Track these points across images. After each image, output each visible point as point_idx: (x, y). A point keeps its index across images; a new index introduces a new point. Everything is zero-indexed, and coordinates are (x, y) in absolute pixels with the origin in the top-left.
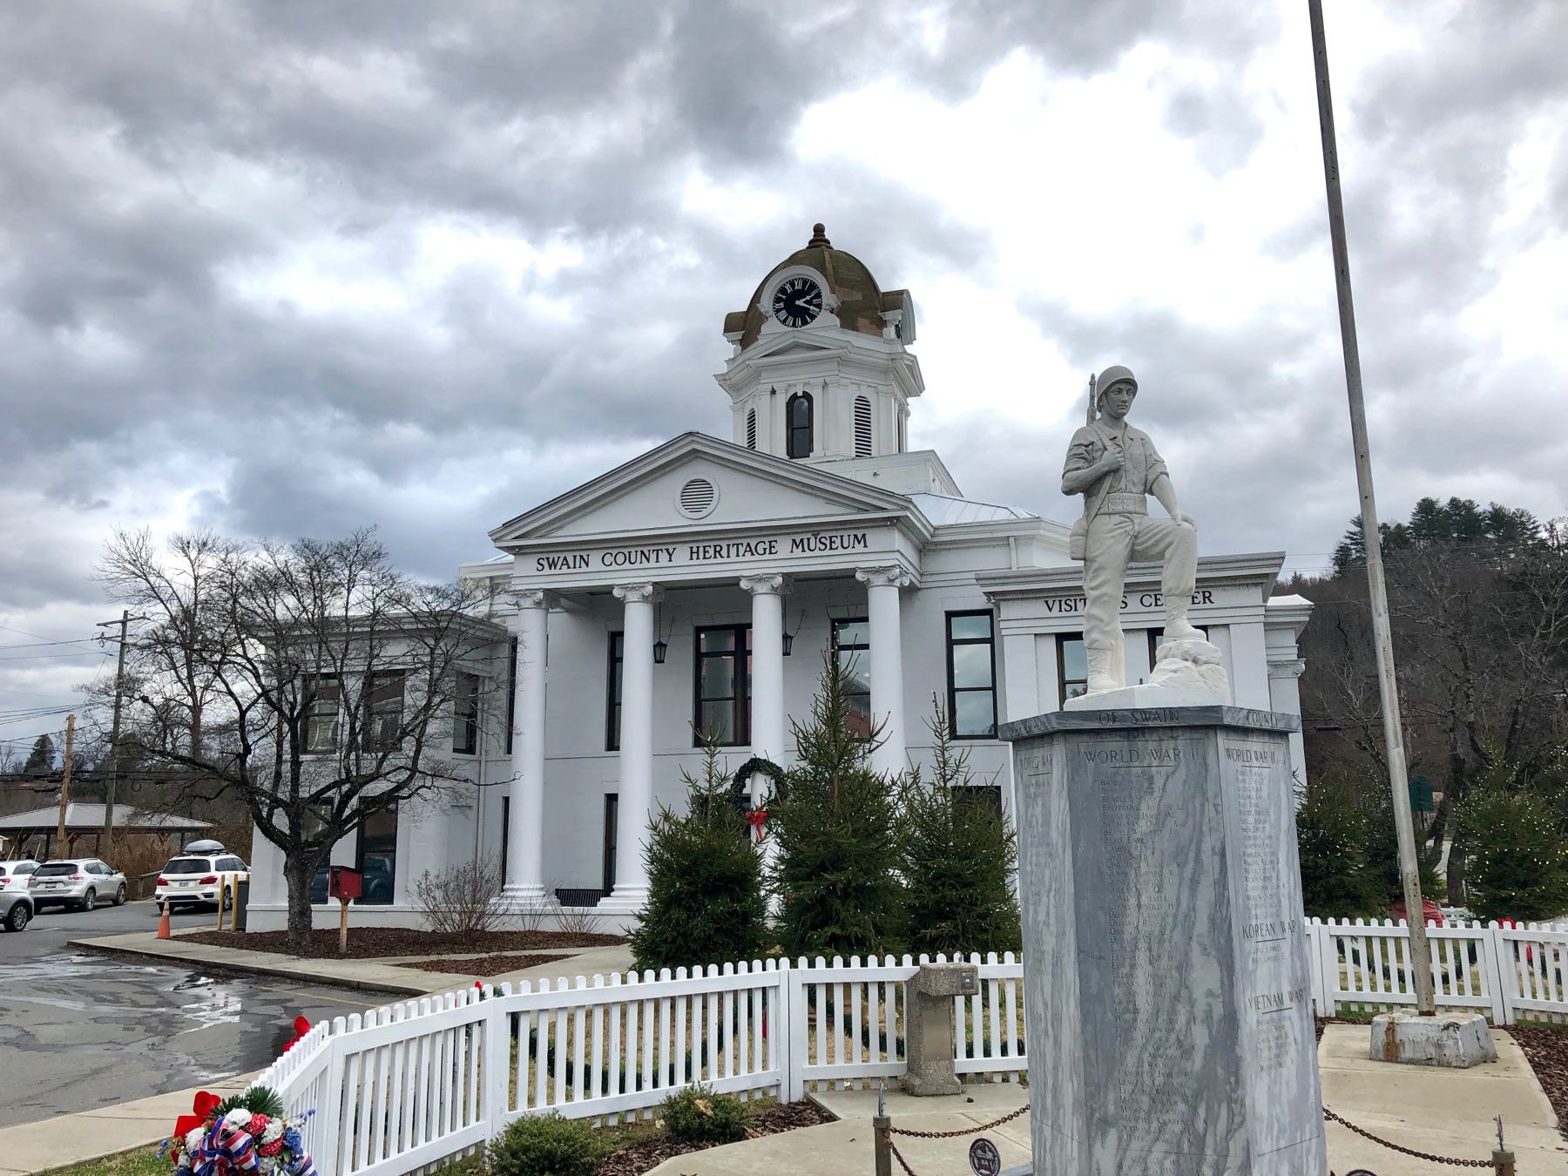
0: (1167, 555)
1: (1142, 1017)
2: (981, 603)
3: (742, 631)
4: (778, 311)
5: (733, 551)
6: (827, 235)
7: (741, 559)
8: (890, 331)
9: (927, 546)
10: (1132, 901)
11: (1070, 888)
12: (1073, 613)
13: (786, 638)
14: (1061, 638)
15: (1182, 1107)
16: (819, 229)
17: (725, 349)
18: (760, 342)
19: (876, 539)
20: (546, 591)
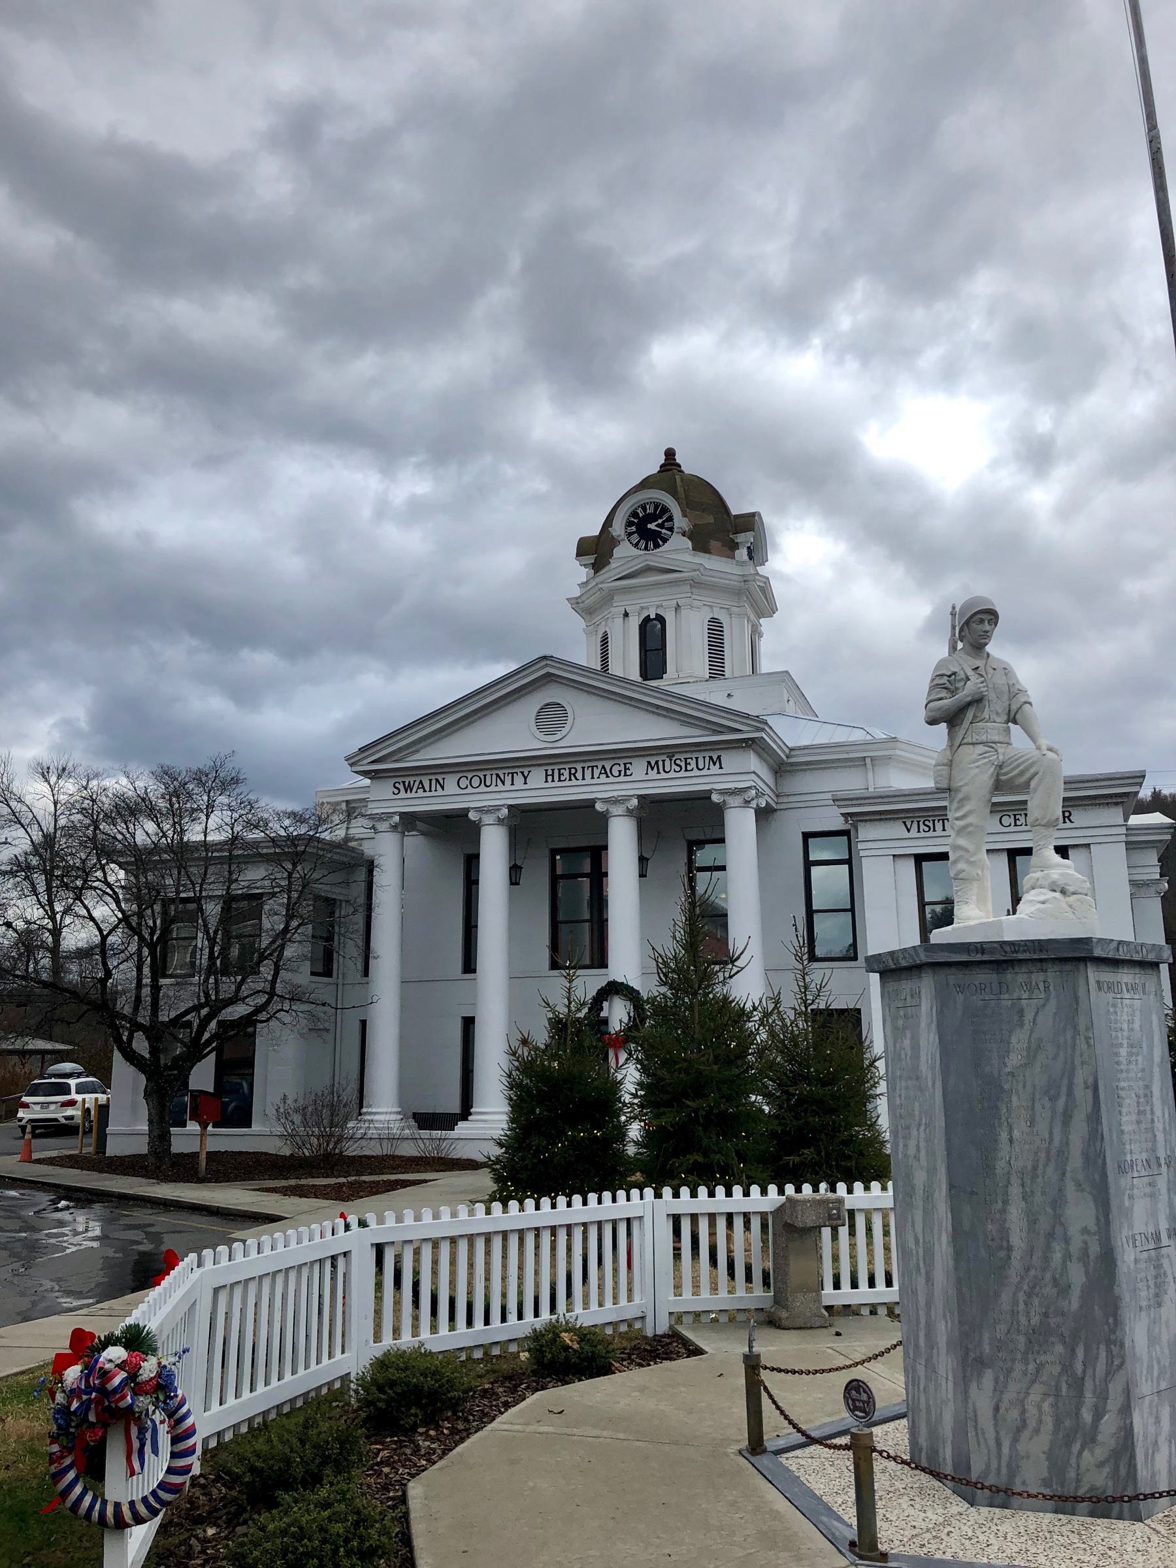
0: (1033, 784)
1: (1016, 1255)
2: (838, 824)
3: (598, 853)
5: (588, 773)
6: (679, 459)
7: (596, 781)
8: (742, 554)
9: (783, 767)
10: (1004, 1136)
11: (940, 1122)
12: (931, 833)
13: (642, 860)
14: (920, 859)
15: (1059, 1348)
16: (670, 454)
17: (580, 573)
18: (613, 565)
19: (733, 761)
20: (402, 815)
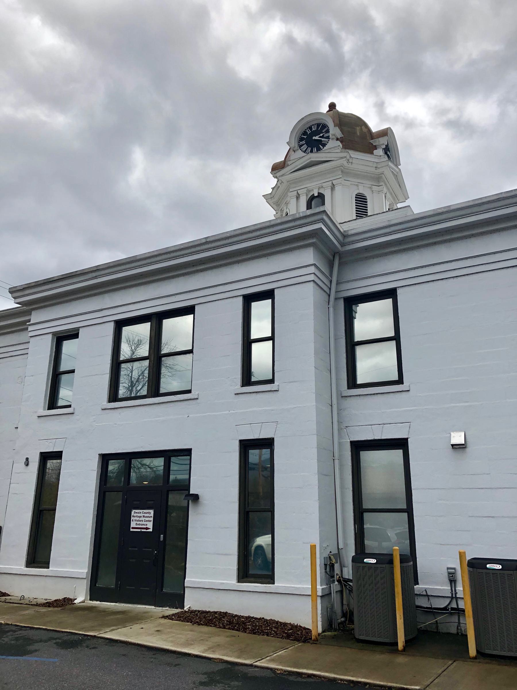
4: (300, 146)
17: (274, 182)
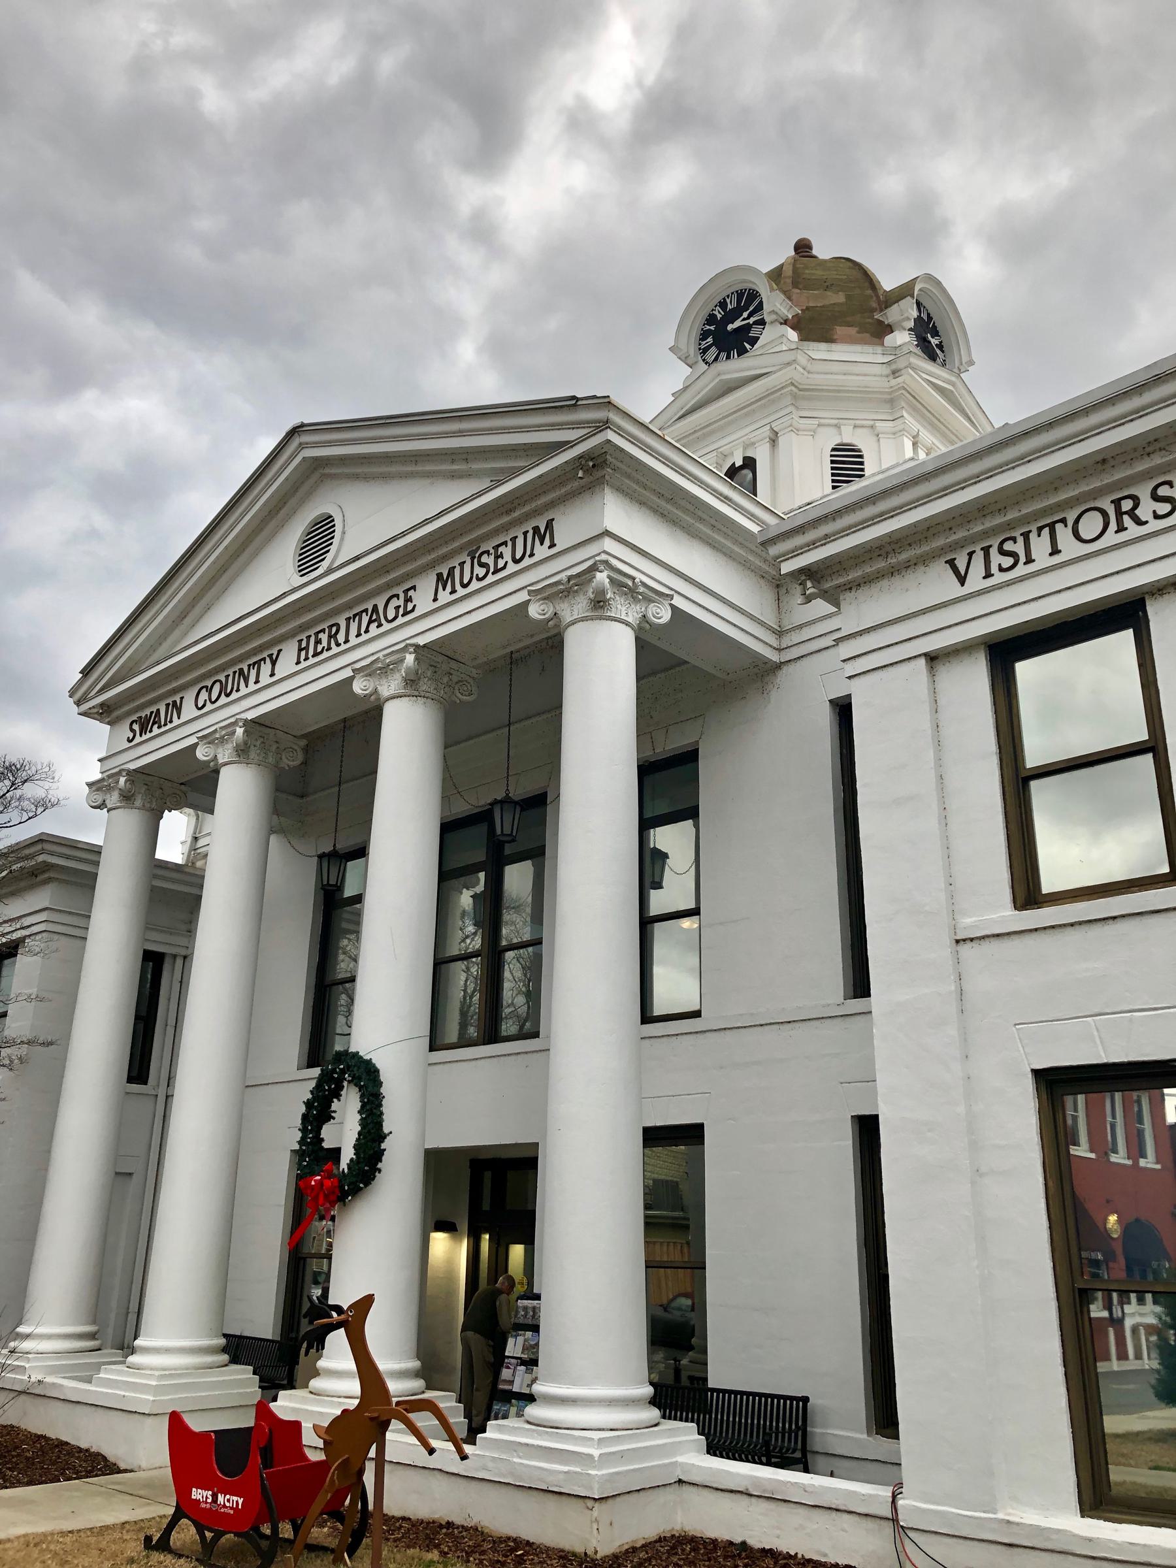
14: (1006, 652)
